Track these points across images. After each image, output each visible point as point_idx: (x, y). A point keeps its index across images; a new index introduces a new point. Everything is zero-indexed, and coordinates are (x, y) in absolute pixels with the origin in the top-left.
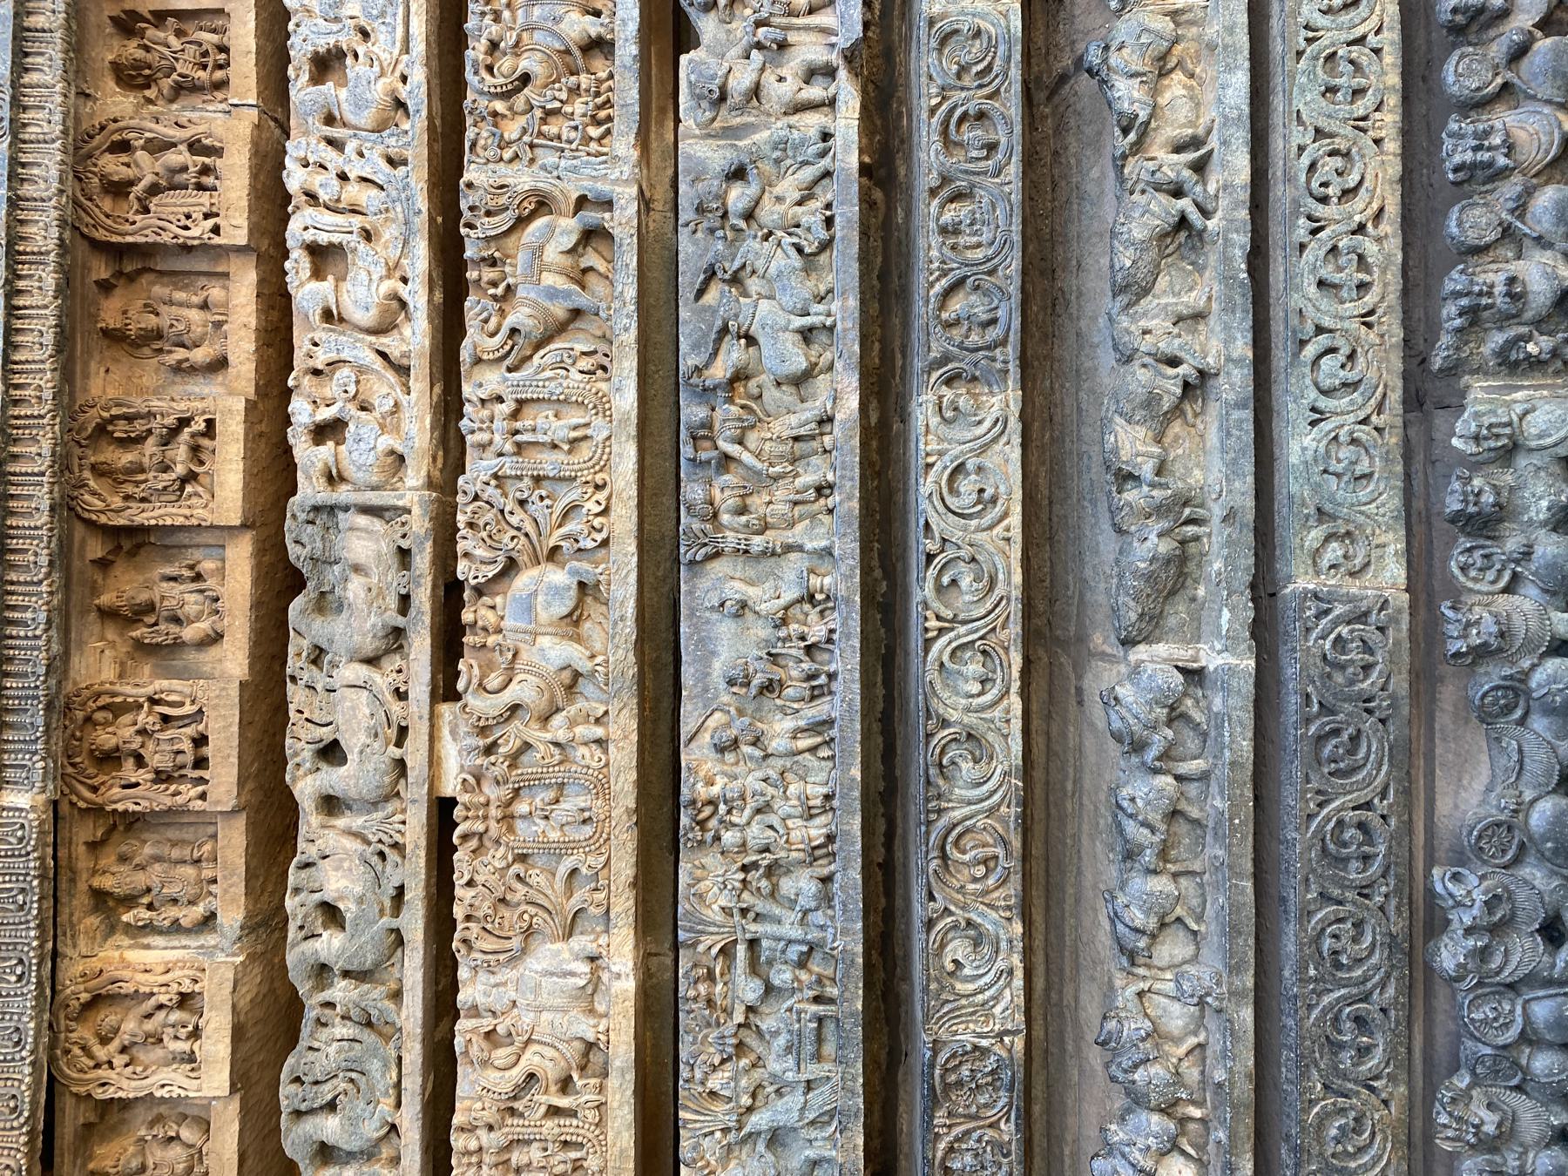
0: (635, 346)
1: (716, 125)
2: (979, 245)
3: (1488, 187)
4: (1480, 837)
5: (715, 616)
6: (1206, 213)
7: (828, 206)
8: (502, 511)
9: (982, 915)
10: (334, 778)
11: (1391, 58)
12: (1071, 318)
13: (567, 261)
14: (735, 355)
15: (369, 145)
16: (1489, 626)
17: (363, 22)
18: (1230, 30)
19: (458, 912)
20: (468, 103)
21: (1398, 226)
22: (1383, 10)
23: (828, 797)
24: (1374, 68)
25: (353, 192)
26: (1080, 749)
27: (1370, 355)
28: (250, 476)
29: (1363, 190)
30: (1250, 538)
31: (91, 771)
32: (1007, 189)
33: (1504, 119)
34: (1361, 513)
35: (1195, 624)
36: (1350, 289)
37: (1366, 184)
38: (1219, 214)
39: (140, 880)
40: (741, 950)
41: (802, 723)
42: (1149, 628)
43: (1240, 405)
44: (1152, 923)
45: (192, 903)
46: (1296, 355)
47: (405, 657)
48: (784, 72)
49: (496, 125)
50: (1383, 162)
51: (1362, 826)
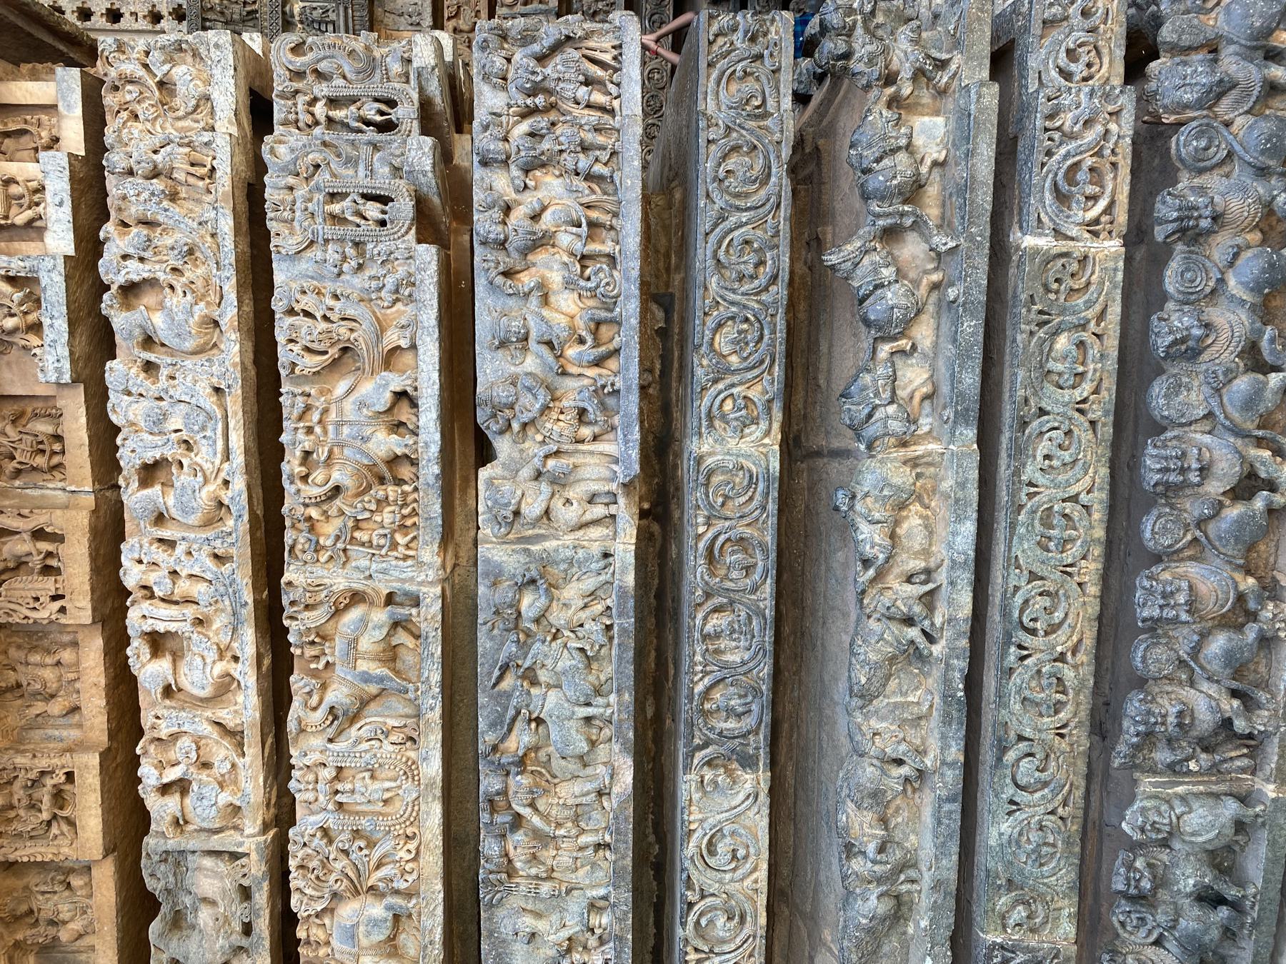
1: (510, 536)
2: (738, 647)
6: (930, 638)
11: (1098, 515)
12: (816, 658)
13: (382, 645)
15: (195, 546)
17: (184, 435)
20: (285, 510)
21: (1092, 656)
25: (184, 587)
29: (1066, 625)
30: (952, 903)
34: (1044, 884)
36: (1049, 707)
37: (1069, 621)
38: (943, 642)
43: (950, 800)
46: (1000, 759)
50: (1085, 603)
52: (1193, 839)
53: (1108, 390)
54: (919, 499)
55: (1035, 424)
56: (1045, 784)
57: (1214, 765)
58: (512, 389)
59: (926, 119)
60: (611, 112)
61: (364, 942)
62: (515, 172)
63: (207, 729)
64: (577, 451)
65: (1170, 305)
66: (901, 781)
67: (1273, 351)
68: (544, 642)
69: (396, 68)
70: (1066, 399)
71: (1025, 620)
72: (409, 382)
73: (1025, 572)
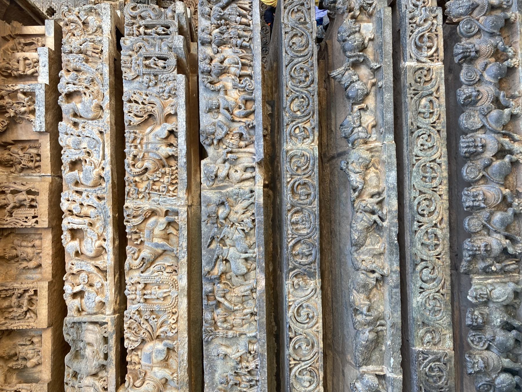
0: (186, 263)
1: (214, 186)
2: (305, 228)
3: (478, 211)
5: (216, 358)
6: (382, 220)
7: (253, 214)
8: (140, 323)
11: (444, 167)
12: (337, 241)
13: (163, 232)
15: (90, 193)
16: (481, 364)
17: (88, 150)
20: (126, 178)
21: (448, 224)
22: (441, 150)
24: (439, 170)
25: (85, 210)
27: (439, 269)
28: (50, 308)
29: (436, 212)
30: (400, 333)
32: (314, 209)
33: (482, 189)
34: (437, 323)
35: (382, 358)
36: (432, 246)
37: (437, 210)
38: (387, 221)
43: (395, 287)
46: (414, 269)
49: (136, 186)
50: (442, 203)
52: (497, 300)
53: (443, 118)
54: (373, 165)
55: (416, 132)
56: (434, 280)
57: (501, 269)
58: (214, 127)
59: (365, 24)
60: (249, 25)
61: (155, 361)
62: (214, 46)
63: (93, 269)
65: (464, 87)
66: (375, 279)
67: (504, 100)
68: (228, 227)
69: (170, 14)
70: (427, 122)
71: (420, 210)
72: (174, 126)
73: (418, 191)
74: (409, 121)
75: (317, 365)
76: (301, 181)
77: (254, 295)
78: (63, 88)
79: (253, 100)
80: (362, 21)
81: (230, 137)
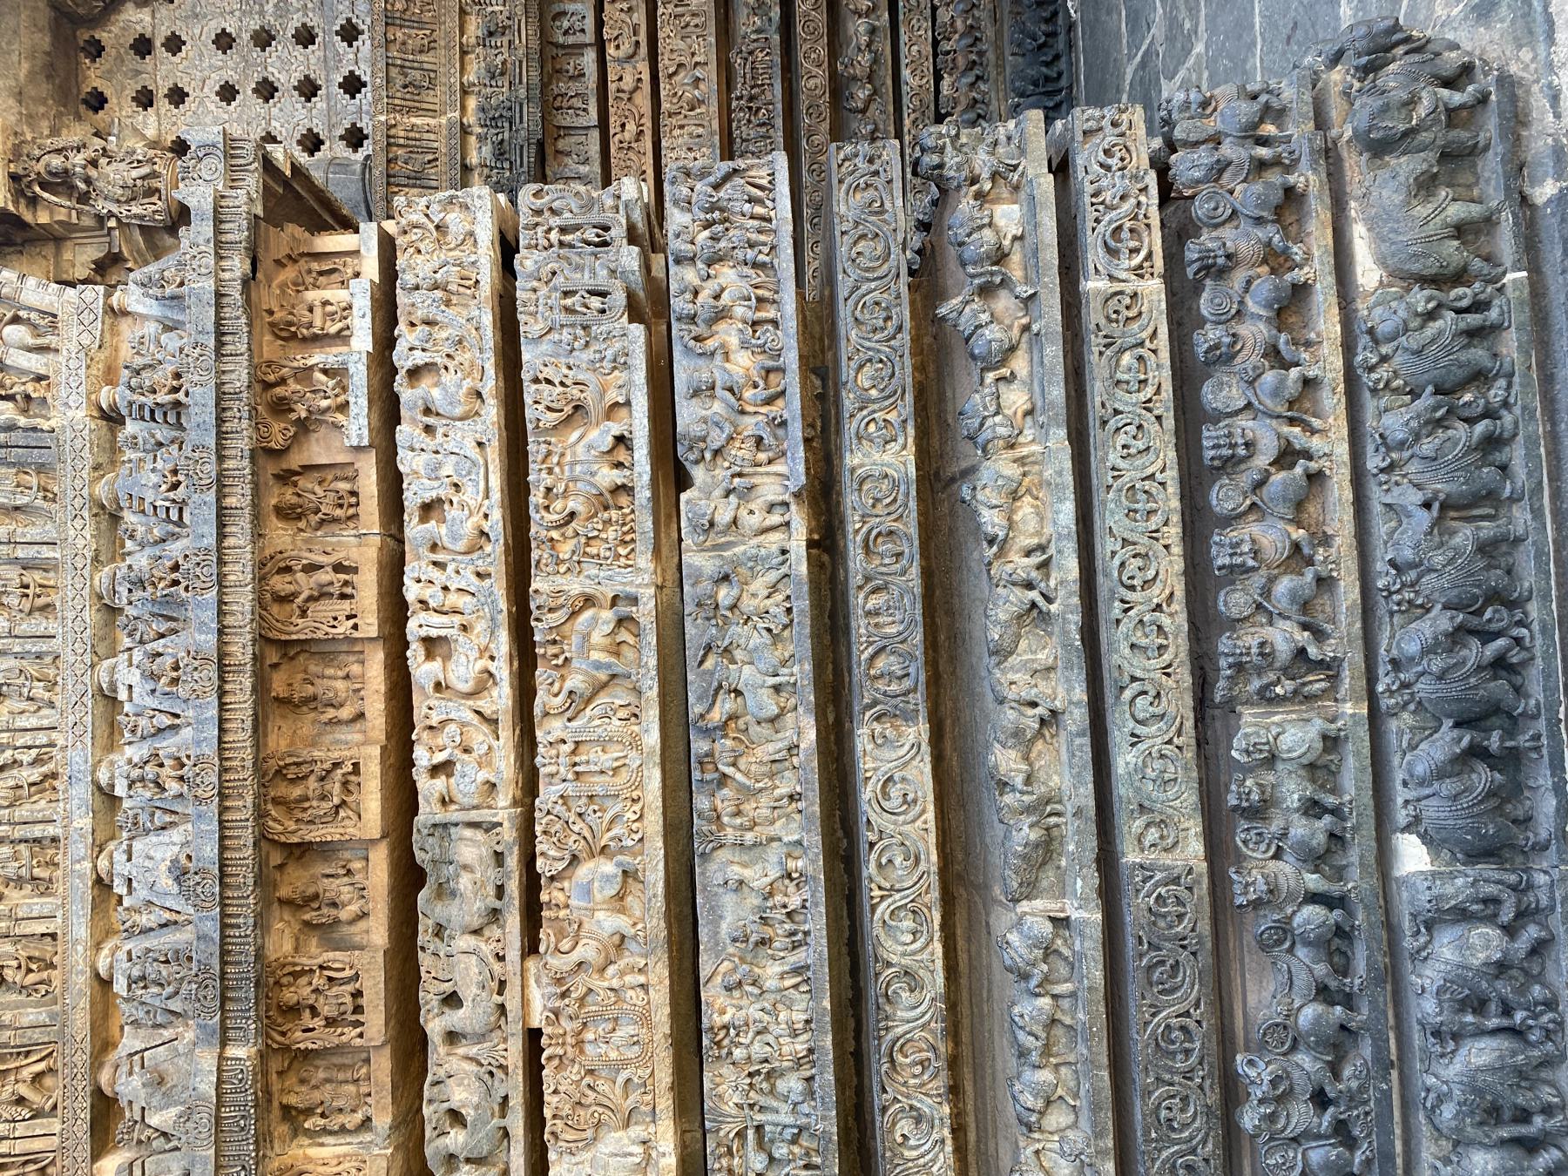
4: (1265, 1034)
5: (721, 890)
6: (1049, 600)
7: (788, 597)
9: (920, 1101)
10: (456, 1019)
11: (1173, 489)
13: (608, 641)
14: (727, 706)
17: (455, 479)
18: (1060, 473)
19: (547, 1113)
23: (807, 1022)
25: (454, 599)
26: (989, 966)
28: (384, 799)
31: (280, 1020)
33: (1251, 529)
39: (317, 1096)
40: (751, 1133)
41: (787, 968)
42: (1030, 889)
43: (1081, 734)
44: (1040, 1104)
45: (353, 1111)
46: (1118, 698)
47: (502, 927)
48: (753, 506)
49: (553, 548)
51: (1183, 1028)
54: (1028, 491)
55: (1112, 422)
57: (1295, 692)
59: (1005, 207)
60: (769, 220)
61: (598, 897)
62: (700, 265)
64: (755, 474)
65: (1208, 326)
69: (609, 202)
71: (1124, 578)
74: (1098, 400)
75: (927, 899)
76: (883, 528)
77: (795, 760)
78: (403, 358)
79: (781, 370)
80: (997, 201)
81: (737, 444)
